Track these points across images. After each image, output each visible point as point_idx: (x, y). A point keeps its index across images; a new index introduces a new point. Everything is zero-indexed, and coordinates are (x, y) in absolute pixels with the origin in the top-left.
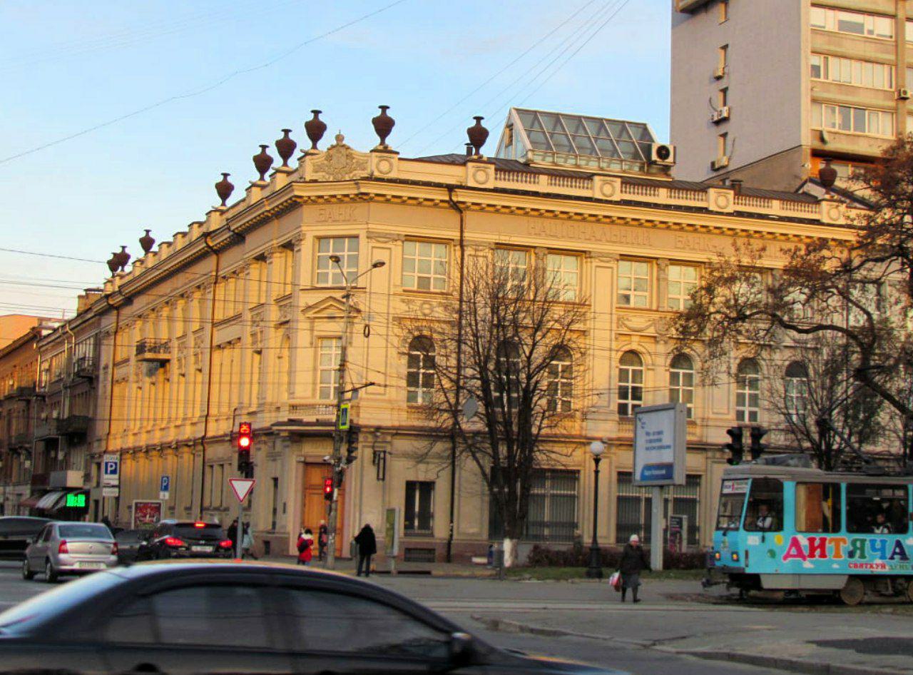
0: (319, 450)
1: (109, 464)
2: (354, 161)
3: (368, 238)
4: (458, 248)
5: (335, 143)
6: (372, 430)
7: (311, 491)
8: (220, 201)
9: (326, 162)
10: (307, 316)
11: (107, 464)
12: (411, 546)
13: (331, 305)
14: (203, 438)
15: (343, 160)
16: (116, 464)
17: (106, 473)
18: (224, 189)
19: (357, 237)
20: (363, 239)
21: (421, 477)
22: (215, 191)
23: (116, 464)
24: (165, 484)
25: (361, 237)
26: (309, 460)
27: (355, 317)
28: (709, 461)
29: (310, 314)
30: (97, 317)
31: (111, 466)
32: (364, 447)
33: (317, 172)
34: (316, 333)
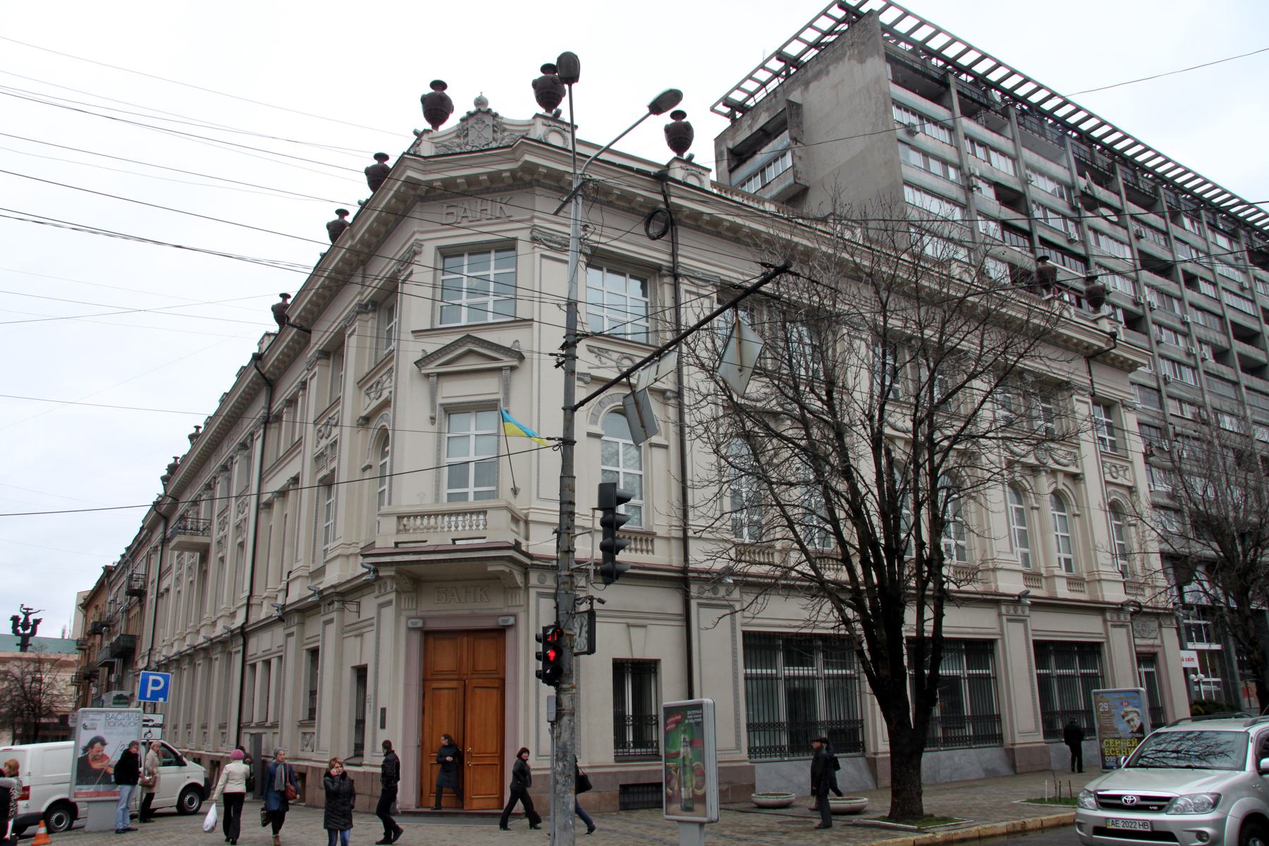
2: (506, 134)
3: (534, 239)
4: (668, 280)
5: (473, 109)
7: (435, 685)
9: (457, 140)
10: (423, 372)
12: (630, 782)
15: (488, 134)
20: (522, 247)
21: (641, 652)
22: (272, 314)
26: (434, 625)
27: (513, 368)
28: (1004, 618)
29: (432, 368)
32: (540, 595)
34: (440, 401)
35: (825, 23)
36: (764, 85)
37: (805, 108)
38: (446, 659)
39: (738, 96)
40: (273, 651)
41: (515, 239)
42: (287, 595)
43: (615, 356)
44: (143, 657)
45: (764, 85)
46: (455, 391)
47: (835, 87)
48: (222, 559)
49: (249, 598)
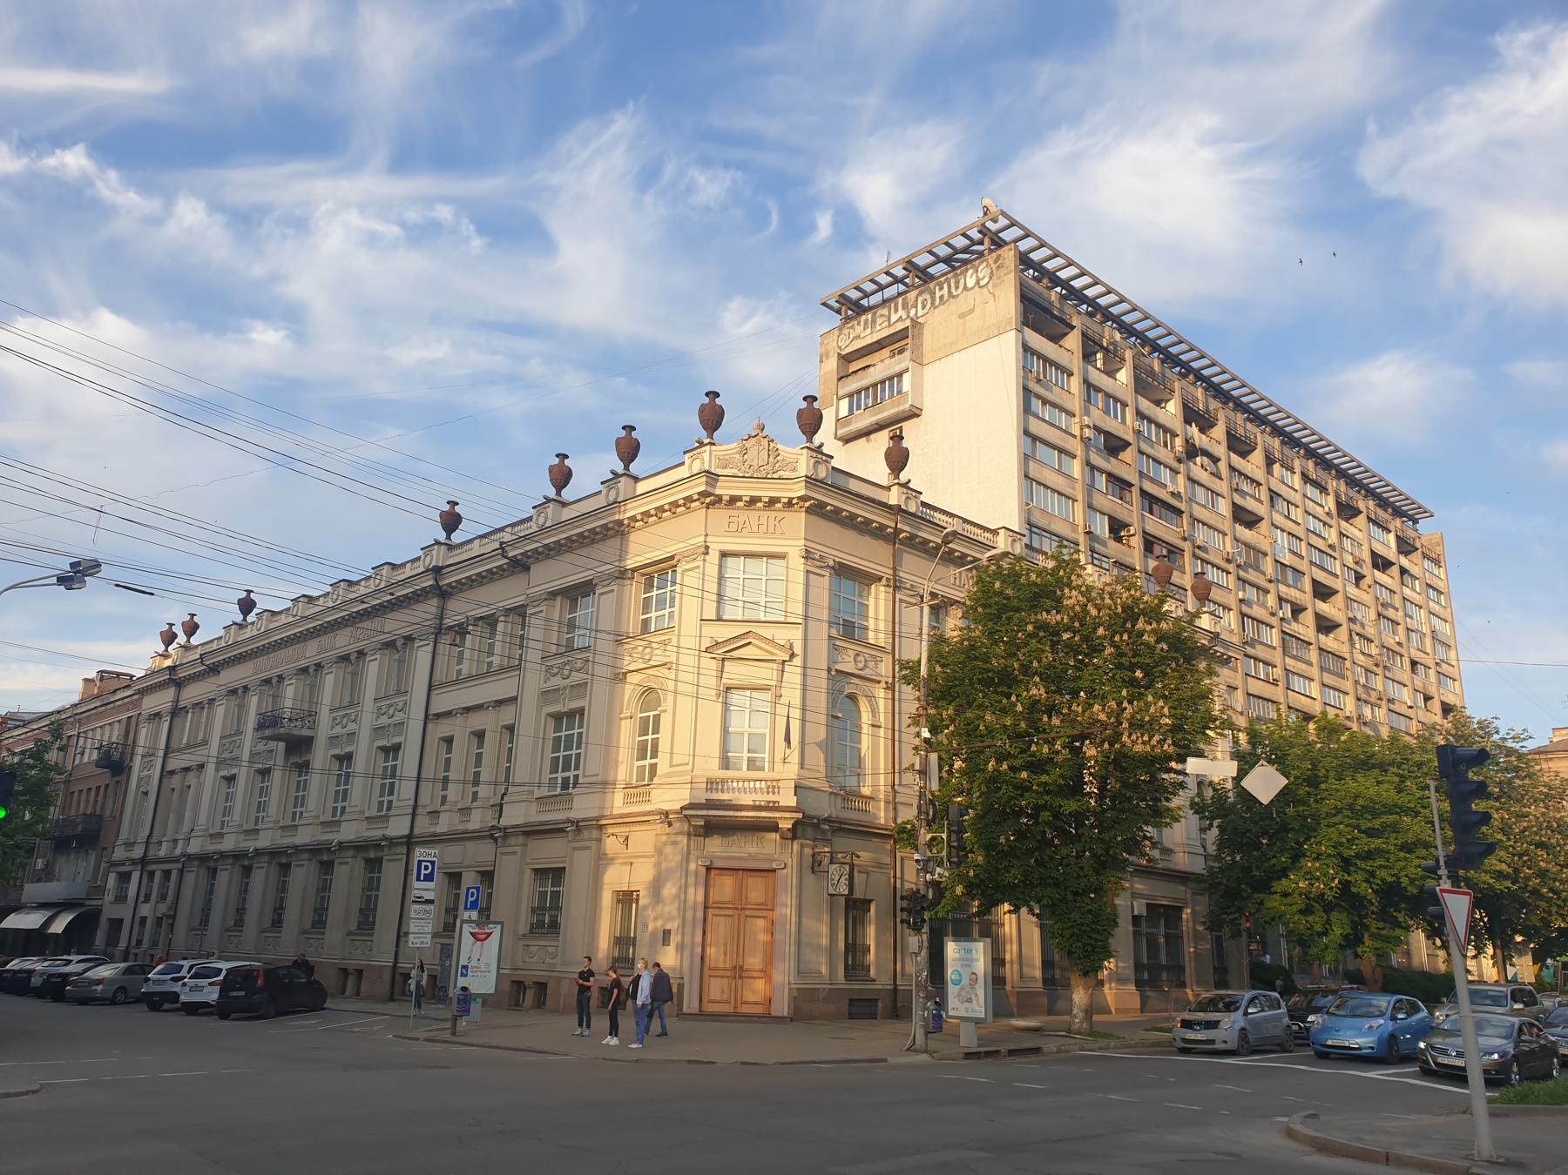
0: (734, 849)
1: (424, 864)
6: (815, 821)
8: (444, 534)
11: (420, 862)
13: (750, 643)
14: (410, 836)
16: (433, 863)
17: (418, 879)
18: (451, 521)
19: (782, 556)
23: (433, 863)
24: (470, 899)
25: (790, 557)
26: (717, 864)
27: (784, 661)
30: (137, 696)
31: (426, 868)
33: (725, 468)
35: (960, 242)
36: (881, 288)
37: (927, 331)
38: (725, 887)
39: (854, 295)
40: (466, 864)
41: (786, 553)
42: (500, 816)
43: (852, 653)
44: (129, 845)
45: (881, 288)
46: (734, 672)
47: (962, 316)
48: (346, 759)
49: (415, 807)
